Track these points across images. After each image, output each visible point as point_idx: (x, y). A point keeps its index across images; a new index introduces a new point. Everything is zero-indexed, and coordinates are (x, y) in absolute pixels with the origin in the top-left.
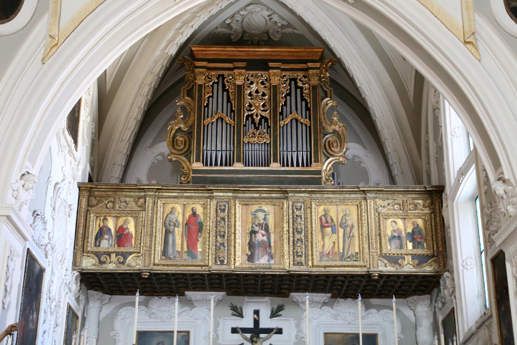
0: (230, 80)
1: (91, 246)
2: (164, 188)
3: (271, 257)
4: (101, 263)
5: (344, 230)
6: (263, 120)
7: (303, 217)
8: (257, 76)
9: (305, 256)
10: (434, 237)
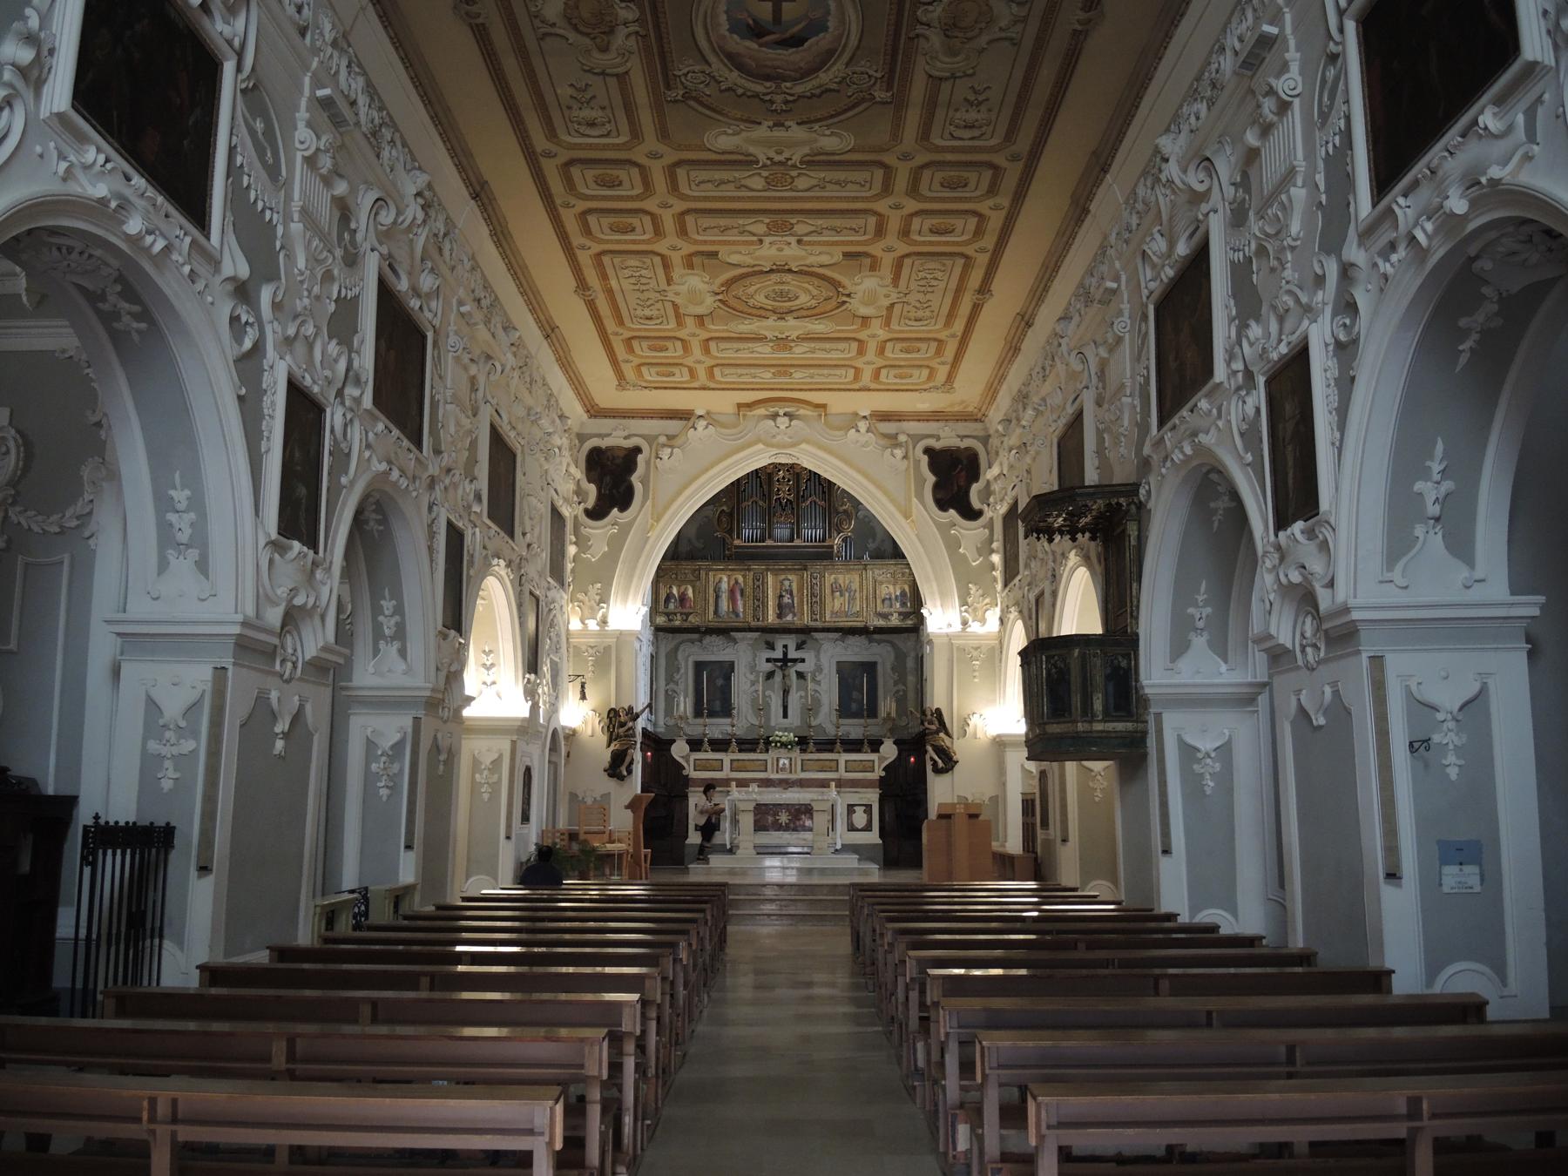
1: (661, 607)
3: (795, 615)
4: (670, 620)
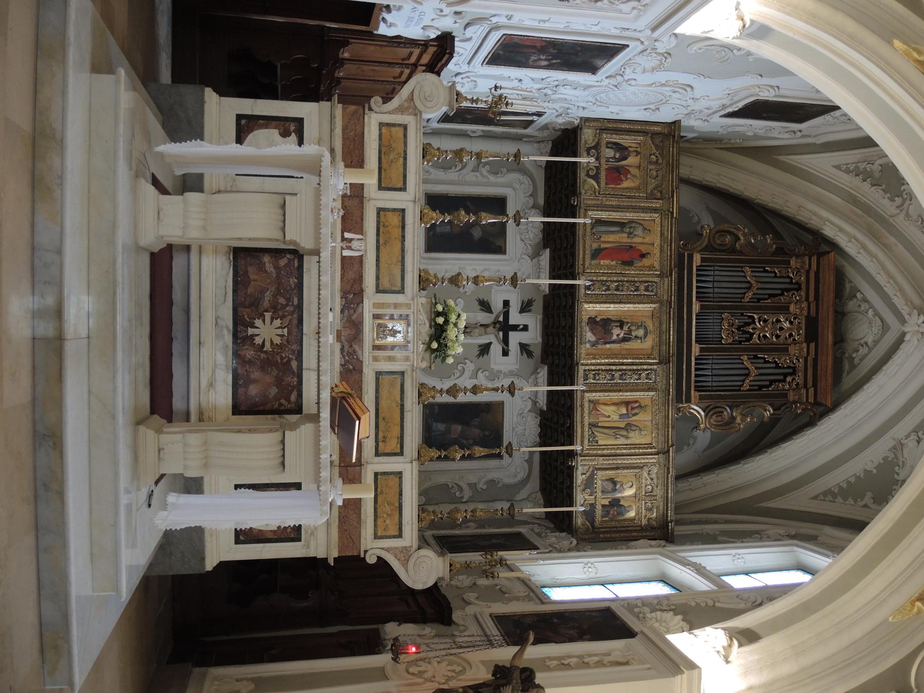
0: (795, 298)
1: (607, 137)
2: (674, 220)
3: (594, 344)
5: (623, 428)
6: (748, 336)
7: (639, 381)
8: (799, 328)
9: (594, 383)
10: (615, 529)
